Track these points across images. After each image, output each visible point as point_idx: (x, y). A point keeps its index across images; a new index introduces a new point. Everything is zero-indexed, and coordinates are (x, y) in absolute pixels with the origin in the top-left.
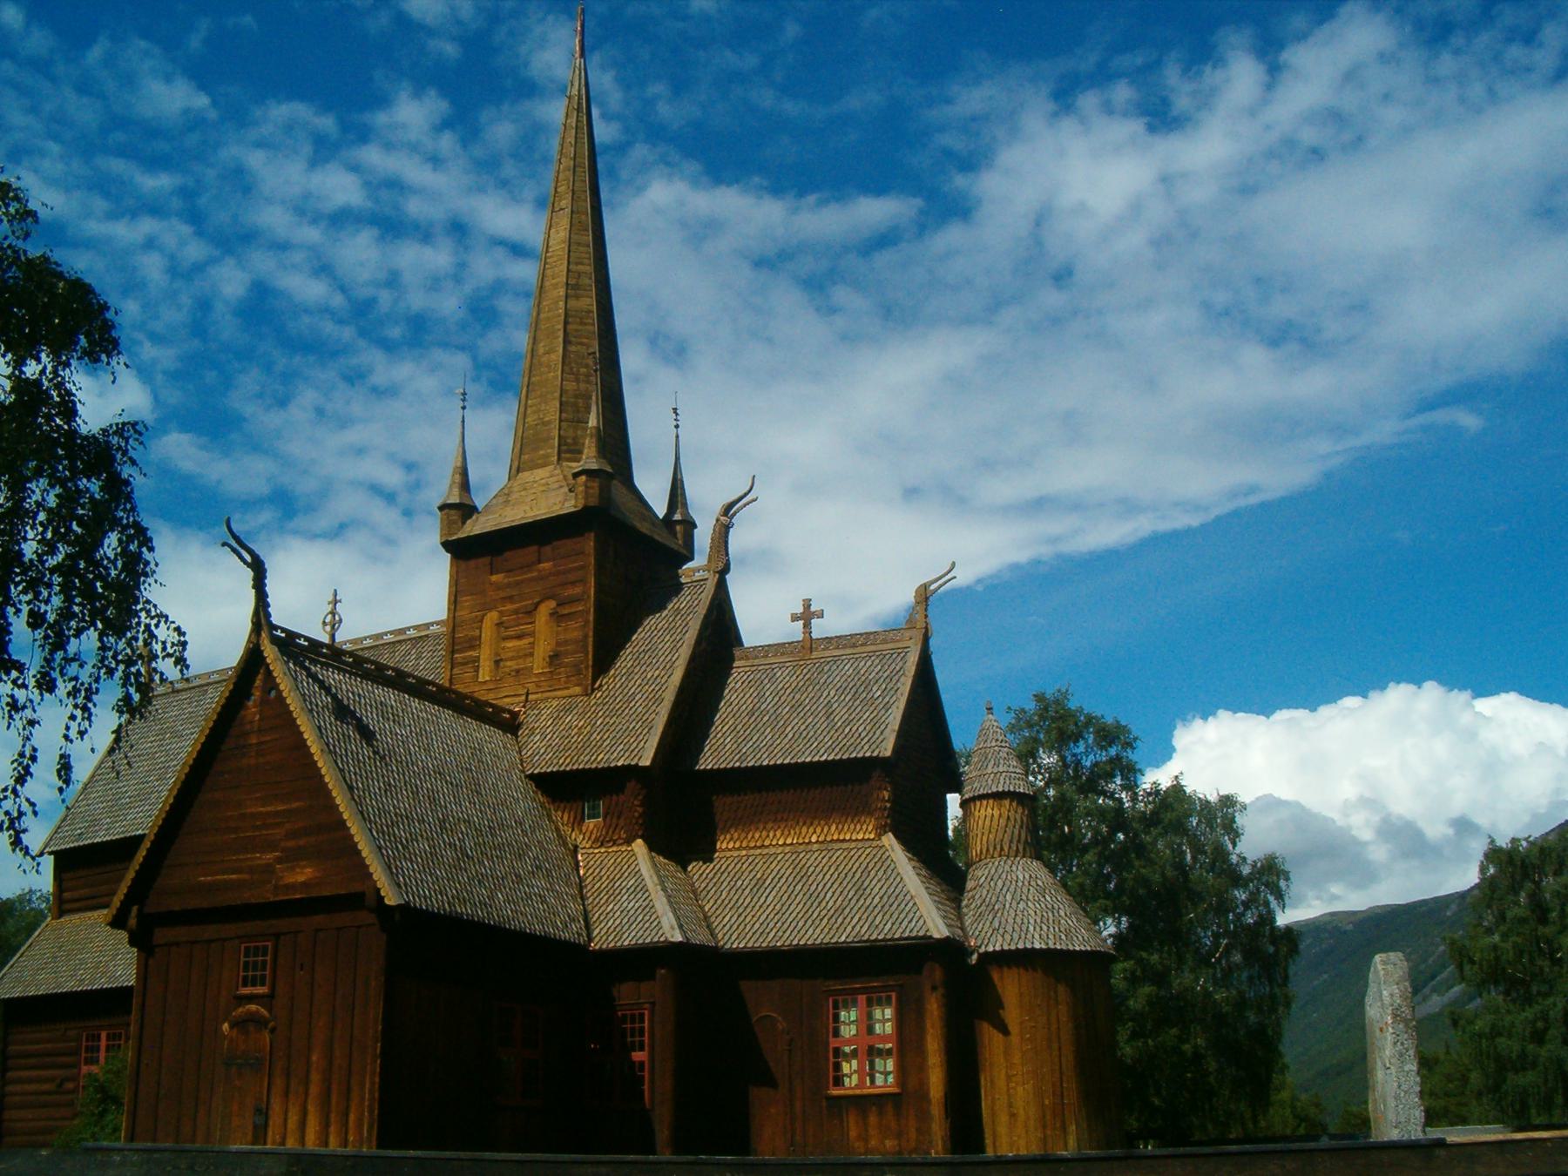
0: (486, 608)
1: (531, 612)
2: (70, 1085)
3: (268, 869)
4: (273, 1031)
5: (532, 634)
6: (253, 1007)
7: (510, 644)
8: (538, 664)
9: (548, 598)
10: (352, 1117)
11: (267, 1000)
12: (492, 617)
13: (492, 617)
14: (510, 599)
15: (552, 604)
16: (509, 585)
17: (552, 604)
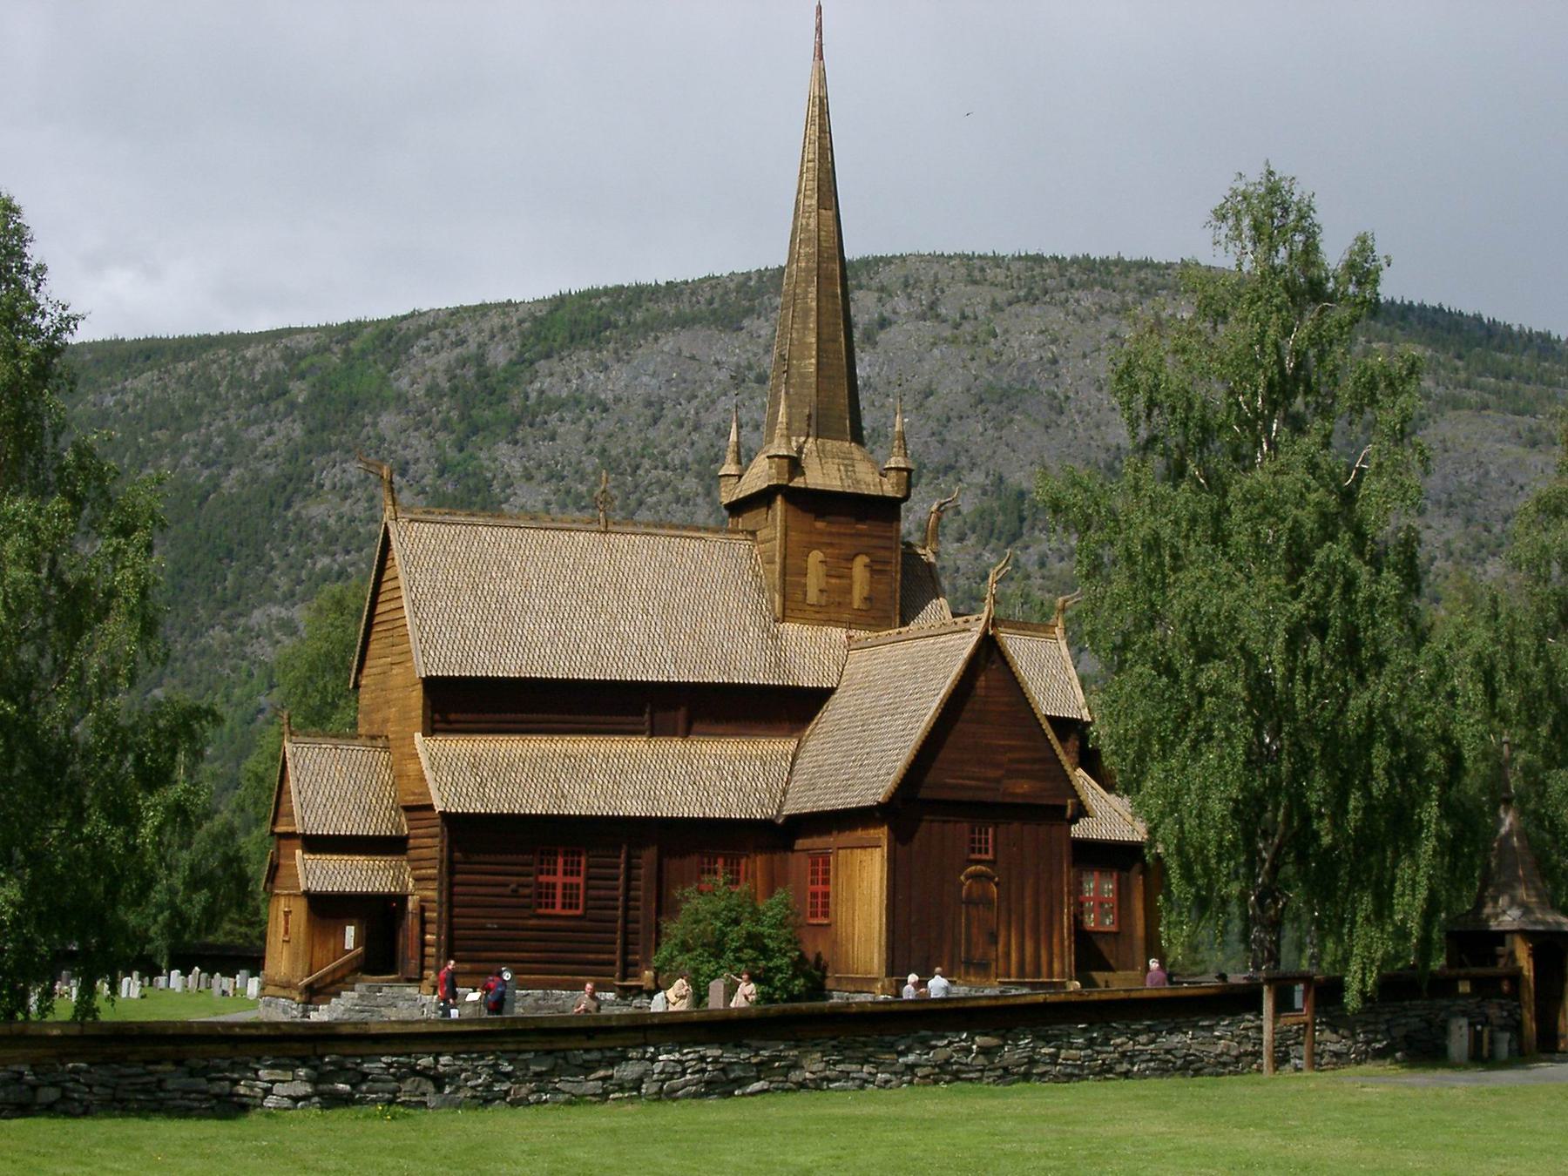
0: (811, 547)
1: (851, 559)
2: (527, 891)
3: (998, 780)
4: (997, 884)
5: (851, 577)
6: (984, 868)
7: (833, 581)
8: (856, 601)
9: (867, 554)
10: (1055, 940)
11: (992, 863)
12: (816, 556)
13: (816, 556)
14: (831, 545)
15: (866, 560)
16: (830, 534)
17: (866, 560)
